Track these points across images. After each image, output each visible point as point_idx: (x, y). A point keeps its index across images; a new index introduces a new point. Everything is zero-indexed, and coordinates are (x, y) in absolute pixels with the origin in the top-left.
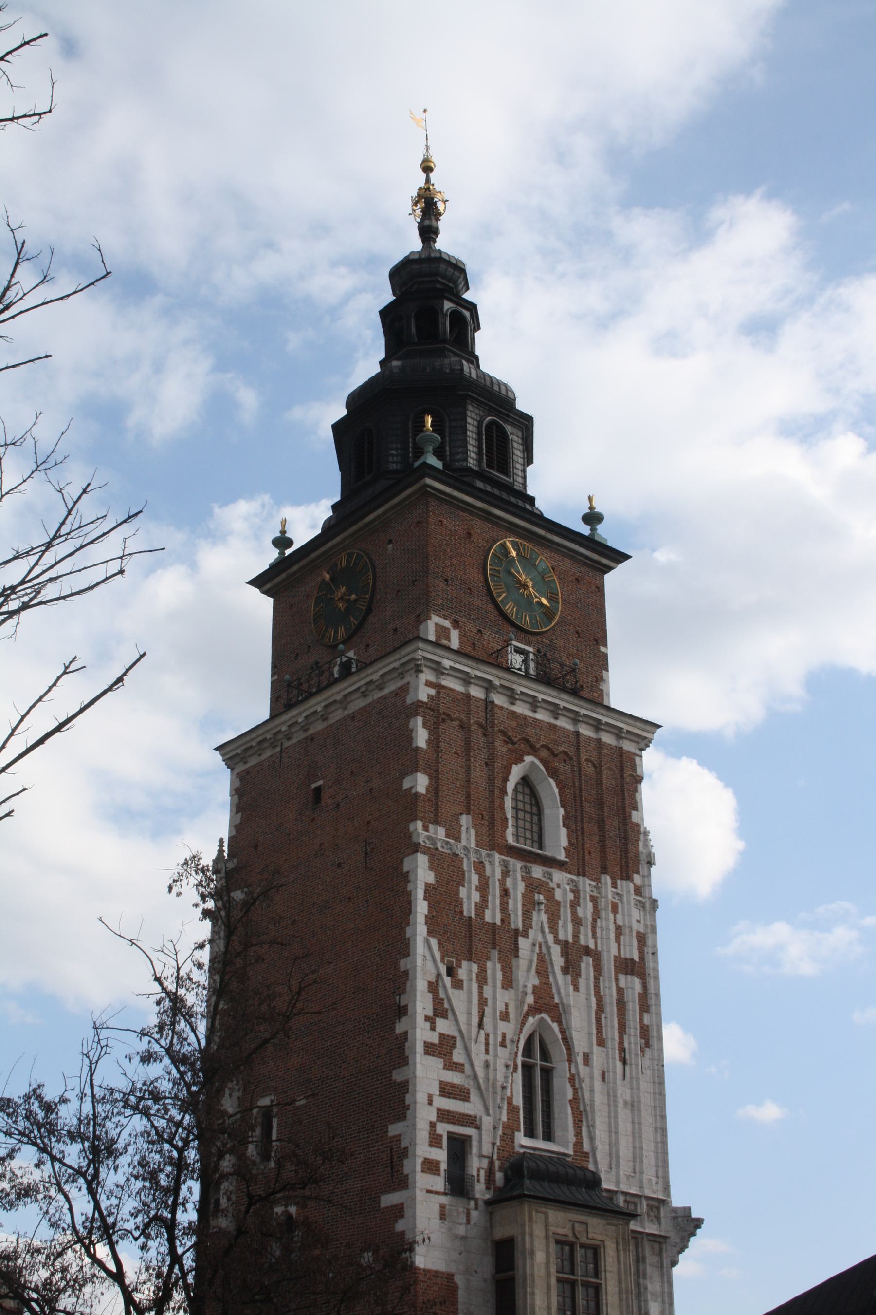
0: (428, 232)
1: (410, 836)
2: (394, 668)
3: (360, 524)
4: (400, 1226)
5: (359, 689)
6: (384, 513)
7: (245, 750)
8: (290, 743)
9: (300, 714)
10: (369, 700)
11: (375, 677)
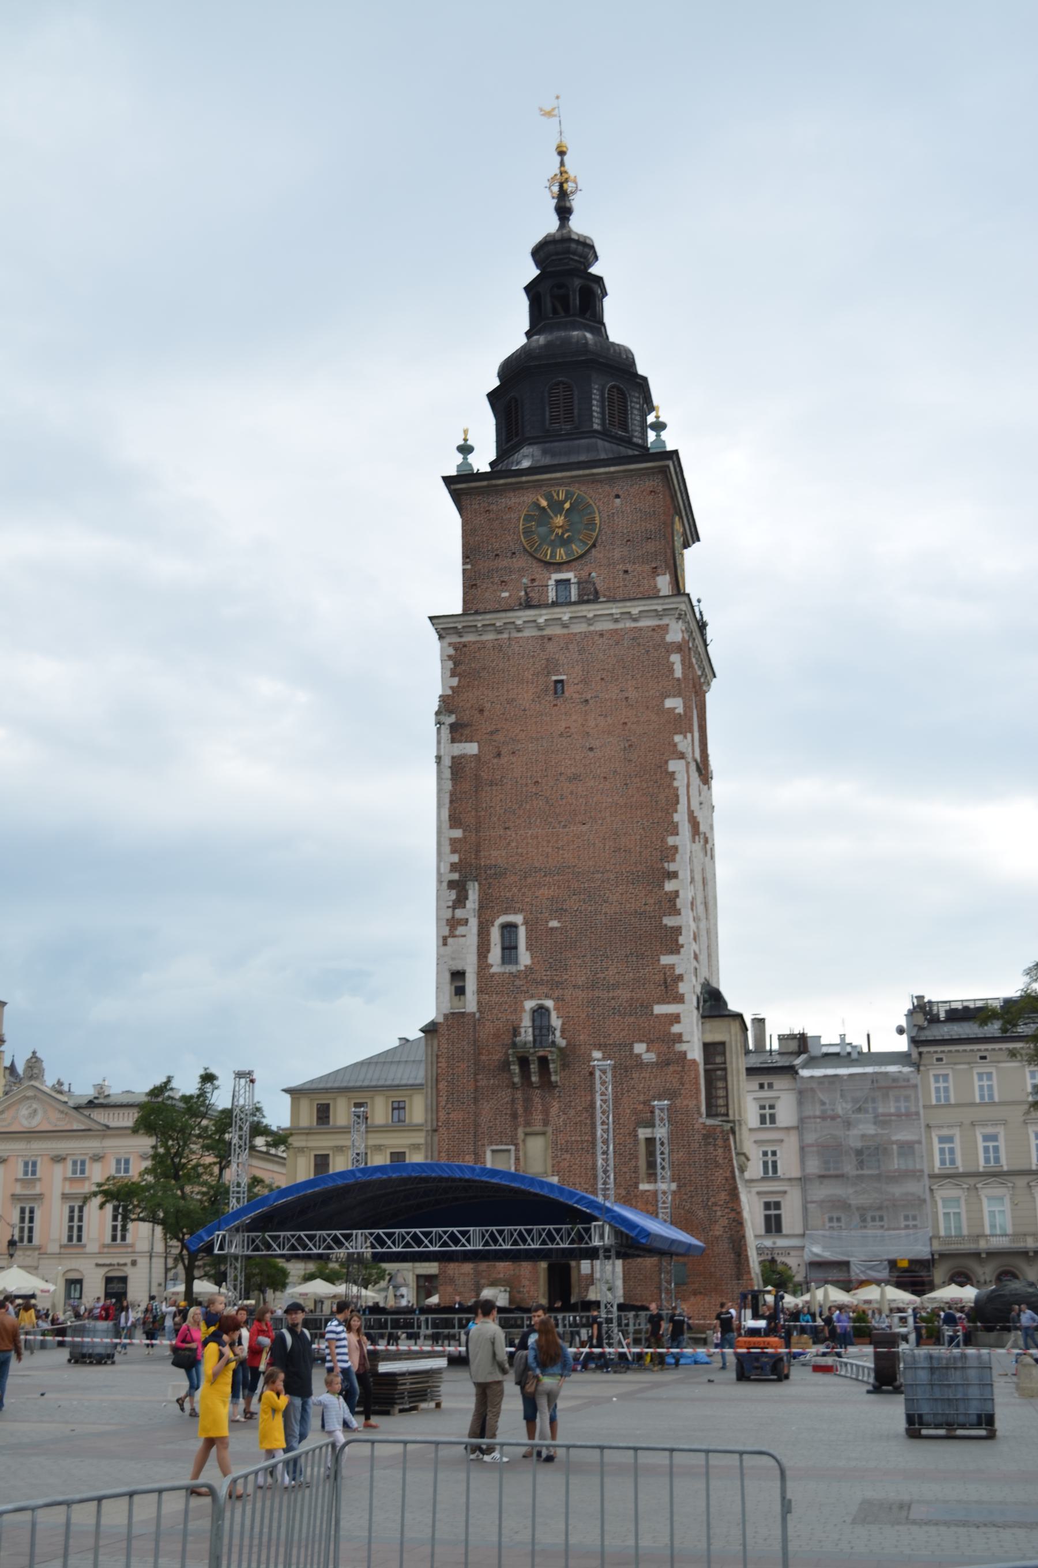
0: (564, 212)
1: (675, 745)
2: (656, 610)
3: (587, 472)
4: (676, 1029)
5: (612, 614)
6: (618, 472)
7: (464, 627)
8: (520, 635)
9: (541, 615)
10: (620, 626)
11: (635, 611)
